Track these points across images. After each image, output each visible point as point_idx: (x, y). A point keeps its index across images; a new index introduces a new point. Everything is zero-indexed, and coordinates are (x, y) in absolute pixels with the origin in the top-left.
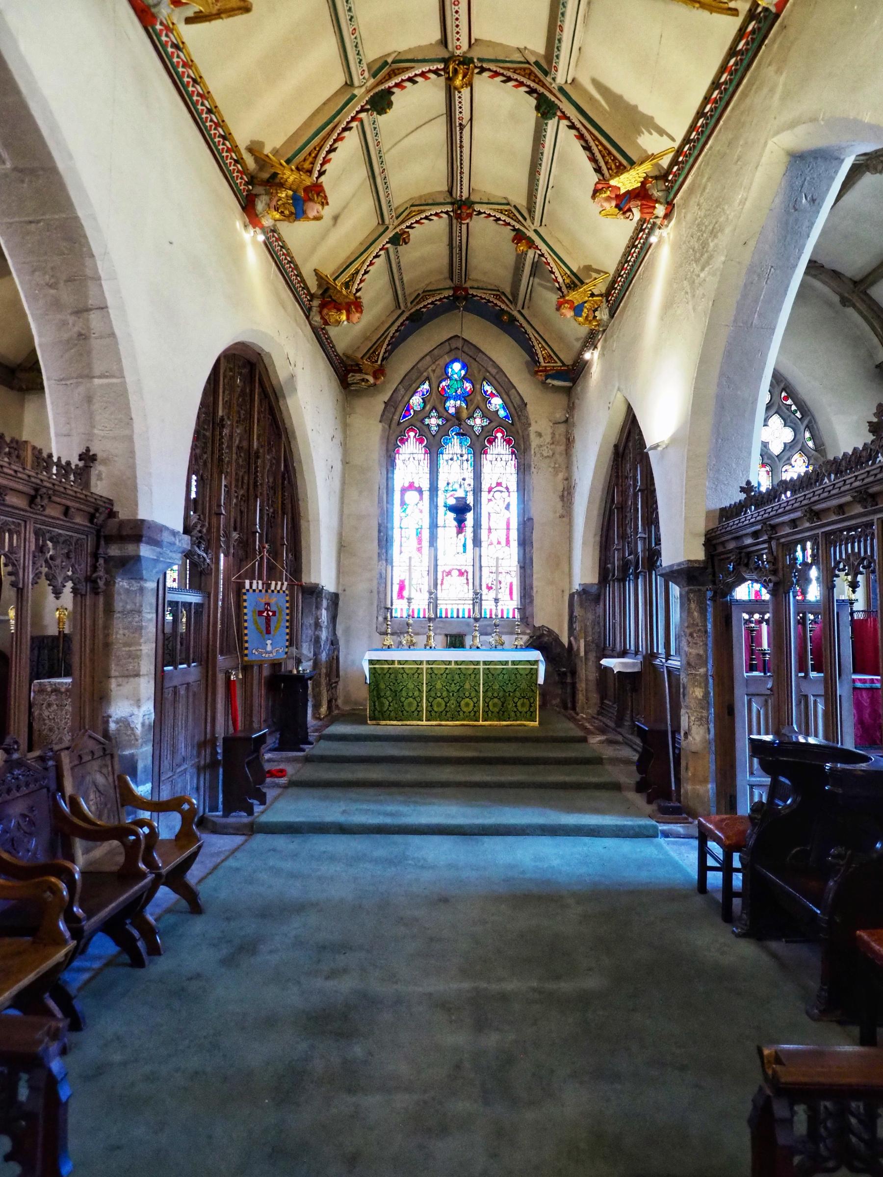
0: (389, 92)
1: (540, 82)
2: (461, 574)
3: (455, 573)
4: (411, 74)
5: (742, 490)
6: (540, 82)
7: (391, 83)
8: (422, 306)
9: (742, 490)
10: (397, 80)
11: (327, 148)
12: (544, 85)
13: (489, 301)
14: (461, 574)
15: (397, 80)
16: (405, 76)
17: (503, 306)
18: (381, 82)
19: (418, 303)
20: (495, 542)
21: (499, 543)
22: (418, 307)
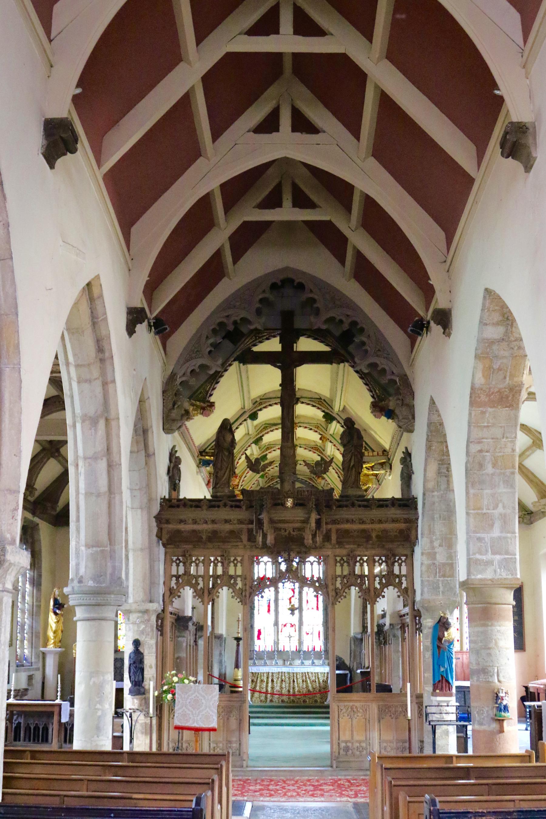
0: (266, 455)
1: (321, 453)
2: (292, 626)
3: (288, 625)
4: (274, 449)
5: (382, 611)
6: (321, 453)
7: (267, 452)
8: (271, 483)
9: (382, 611)
10: (270, 451)
11: (244, 476)
12: (323, 454)
13: (306, 481)
14: (292, 626)
15: (270, 451)
16: (273, 449)
17: (314, 484)
18: (263, 452)
19: (269, 483)
20: (310, 608)
21: (313, 608)
22: (269, 484)
